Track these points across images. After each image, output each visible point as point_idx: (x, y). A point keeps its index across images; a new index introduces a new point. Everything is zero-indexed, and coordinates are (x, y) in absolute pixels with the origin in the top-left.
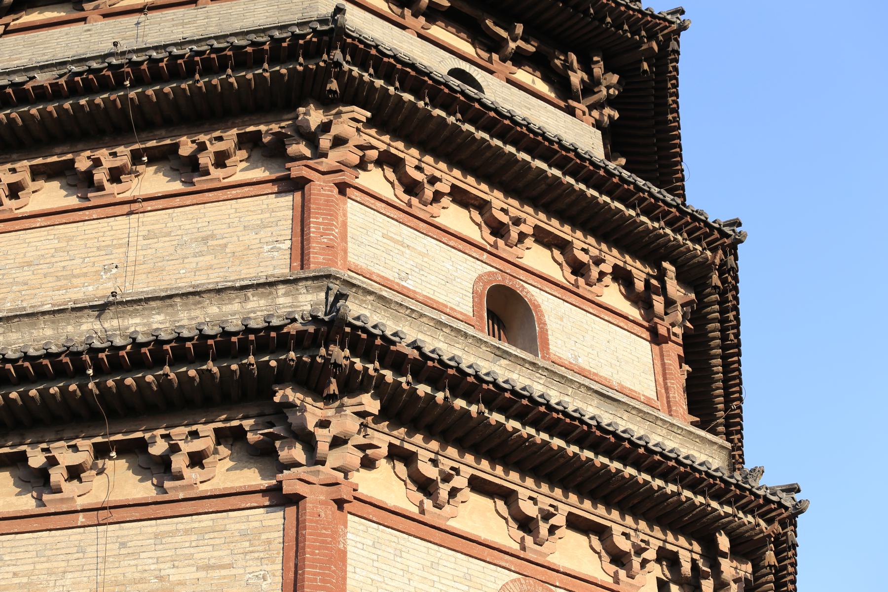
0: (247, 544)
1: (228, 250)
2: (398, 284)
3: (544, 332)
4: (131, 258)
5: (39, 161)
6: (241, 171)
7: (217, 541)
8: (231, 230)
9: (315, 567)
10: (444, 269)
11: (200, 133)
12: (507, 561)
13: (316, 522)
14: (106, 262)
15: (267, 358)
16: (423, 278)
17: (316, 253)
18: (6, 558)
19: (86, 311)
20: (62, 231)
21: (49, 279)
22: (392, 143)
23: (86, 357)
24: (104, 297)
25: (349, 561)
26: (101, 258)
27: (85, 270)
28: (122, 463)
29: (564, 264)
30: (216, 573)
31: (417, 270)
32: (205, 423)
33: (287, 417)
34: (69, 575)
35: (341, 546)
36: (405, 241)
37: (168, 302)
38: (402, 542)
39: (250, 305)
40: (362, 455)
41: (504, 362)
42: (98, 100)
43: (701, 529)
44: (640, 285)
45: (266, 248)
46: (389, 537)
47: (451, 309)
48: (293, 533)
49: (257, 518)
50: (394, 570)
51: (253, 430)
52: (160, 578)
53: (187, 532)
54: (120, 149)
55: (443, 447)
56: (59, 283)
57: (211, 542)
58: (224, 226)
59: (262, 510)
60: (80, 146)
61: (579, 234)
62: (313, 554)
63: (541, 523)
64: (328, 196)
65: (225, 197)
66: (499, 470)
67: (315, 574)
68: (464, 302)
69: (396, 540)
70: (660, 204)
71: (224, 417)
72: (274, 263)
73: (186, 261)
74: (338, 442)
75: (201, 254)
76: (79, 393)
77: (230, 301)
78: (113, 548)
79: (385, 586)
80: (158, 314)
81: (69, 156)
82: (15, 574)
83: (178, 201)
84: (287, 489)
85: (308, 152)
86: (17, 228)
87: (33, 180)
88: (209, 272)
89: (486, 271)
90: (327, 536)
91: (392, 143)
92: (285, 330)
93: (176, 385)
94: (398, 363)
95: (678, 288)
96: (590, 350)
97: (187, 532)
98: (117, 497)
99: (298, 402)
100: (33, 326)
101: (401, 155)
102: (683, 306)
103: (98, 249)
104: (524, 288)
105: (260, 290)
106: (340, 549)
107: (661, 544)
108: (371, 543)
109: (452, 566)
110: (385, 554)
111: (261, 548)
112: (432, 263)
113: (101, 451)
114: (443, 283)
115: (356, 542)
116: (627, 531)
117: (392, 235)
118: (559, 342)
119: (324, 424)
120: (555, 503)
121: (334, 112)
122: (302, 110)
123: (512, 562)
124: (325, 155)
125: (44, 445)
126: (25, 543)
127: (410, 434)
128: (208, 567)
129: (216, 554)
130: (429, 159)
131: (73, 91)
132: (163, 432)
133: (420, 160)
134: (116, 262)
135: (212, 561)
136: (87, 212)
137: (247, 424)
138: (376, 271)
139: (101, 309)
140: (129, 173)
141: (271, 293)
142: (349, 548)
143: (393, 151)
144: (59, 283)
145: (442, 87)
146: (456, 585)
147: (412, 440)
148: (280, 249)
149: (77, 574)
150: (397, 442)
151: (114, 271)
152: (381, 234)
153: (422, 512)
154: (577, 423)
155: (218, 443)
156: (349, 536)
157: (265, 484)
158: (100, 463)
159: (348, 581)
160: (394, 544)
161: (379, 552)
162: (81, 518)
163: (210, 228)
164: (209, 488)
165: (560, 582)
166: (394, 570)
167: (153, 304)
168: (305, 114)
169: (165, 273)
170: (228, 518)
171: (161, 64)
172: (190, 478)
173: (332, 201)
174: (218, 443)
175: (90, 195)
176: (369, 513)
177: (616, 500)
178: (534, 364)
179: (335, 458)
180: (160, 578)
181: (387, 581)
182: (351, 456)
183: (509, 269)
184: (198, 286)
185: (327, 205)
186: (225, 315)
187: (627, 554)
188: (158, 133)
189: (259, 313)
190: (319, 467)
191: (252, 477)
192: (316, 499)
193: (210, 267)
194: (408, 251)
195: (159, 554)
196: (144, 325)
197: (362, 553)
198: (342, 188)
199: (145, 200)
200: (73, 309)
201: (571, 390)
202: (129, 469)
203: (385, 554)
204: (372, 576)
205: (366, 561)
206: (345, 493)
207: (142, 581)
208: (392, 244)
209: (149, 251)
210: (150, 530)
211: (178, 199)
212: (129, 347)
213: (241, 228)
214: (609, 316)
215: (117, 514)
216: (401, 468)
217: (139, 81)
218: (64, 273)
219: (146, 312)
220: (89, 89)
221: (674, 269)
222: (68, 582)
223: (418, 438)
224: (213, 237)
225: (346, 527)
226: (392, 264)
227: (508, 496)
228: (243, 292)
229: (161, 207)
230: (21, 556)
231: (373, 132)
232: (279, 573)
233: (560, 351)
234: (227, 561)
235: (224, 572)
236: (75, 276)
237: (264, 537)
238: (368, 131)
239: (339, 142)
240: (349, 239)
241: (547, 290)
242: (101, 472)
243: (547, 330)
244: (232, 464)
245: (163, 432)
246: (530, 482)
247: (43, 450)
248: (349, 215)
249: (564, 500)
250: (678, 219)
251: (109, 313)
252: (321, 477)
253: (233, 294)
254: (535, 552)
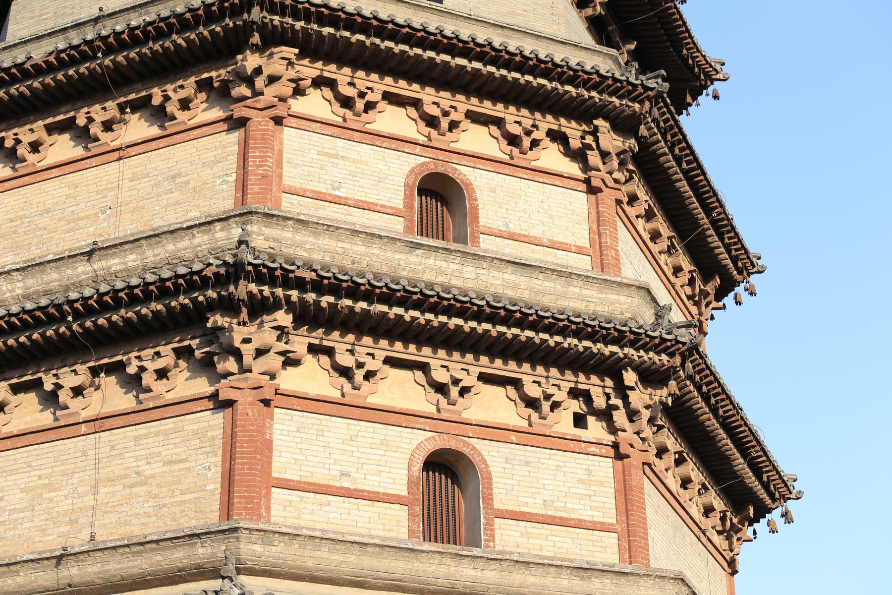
0: (198, 441)
1: (190, 186)
2: (330, 195)
3: (475, 208)
4: (119, 200)
5: (50, 120)
6: (203, 111)
7: (177, 440)
8: (193, 167)
9: (243, 458)
10: (376, 170)
11: (167, 83)
12: (422, 424)
13: (245, 421)
14: (103, 205)
15: (196, 294)
16: (356, 183)
17: (253, 185)
18: (34, 464)
19: (79, 257)
20: (71, 179)
21: (63, 223)
22: (324, 68)
23: (66, 307)
24: (89, 245)
25: (274, 447)
26: (99, 201)
27: (87, 213)
28: (112, 379)
29: (500, 138)
30: (176, 467)
31: (350, 177)
32: (165, 345)
33: (219, 338)
34: (76, 475)
35: (268, 437)
36: (340, 153)
37: (137, 244)
38: (324, 423)
39: (197, 241)
40: (283, 359)
41: (418, 252)
42: (82, 70)
43: (611, 369)
44: (575, 144)
45: (218, 181)
46: (312, 421)
47: (382, 206)
48: (229, 430)
49: (205, 419)
50: (316, 448)
52: (138, 473)
53: (157, 434)
54: (110, 104)
55: (359, 339)
56: (69, 226)
57: (173, 441)
58: (188, 164)
59: (209, 412)
60: (79, 104)
61: (512, 109)
62: (242, 447)
63: (451, 387)
64: (265, 130)
65: (189, 138)
66: (412, 348)
67: (244, 464)
68: (396, 196)
69: (318, 422)
70: (581, 73)
71: (178, 338)
72: (224, 194)
73: (160, 198)
74: (260, 353)
75: (170, 191)
76: (68, 333)
77: (182, 238)
78: (105, 451)
79: (307, 463)
80: (131, 254)
81: (72, 114)
82: (40, 477)
83: (154, 144)
84: (222, 396)
85: (247, 92)
86: (38, 179)
87: (50, 135)
88: (176, 207)
89: (419, 162)
90: (253, 431)
91: (324, 68)
92: (204, 273)
93: (136, 321)
94: (301, 284)
95: (615, 137)
96: (522, 214)
97: (157, 434)
98: (108, 410)
99: (226, 325)
100: (43, 272)
101: (333, 76)
102: (618, 155)
103: (97, 193)
104: (455, 169)
105: (202, 228)
106: (266, 440)
107: (573, 385)
108: (295, 429)
109: (371, 435)
110: (309, 436)
111: (207, 444)
112: (364, 167)
113: (95, 372)
114: (375, 183)
115: (282, 430)
116: (538, 379)
117: (327, 151)
118: (491, 213)
119: (247, 341)
120: (466, 367)
121: (267, 53)
122: (239, 57)
123: (426, 424)
124: (262, 94)
125: (54, 372)
126: (46, 451)
127: (327, 333)
128: (172, 462)
129: (176, 451)
130: (361, 74)
131: (63, 65)
132: (136, 354)
133: (352, 77)
134: (109, 204)
135: (174, 457)
136: (88, 161)
137: (194, 343)
138: (310, 188)
139: (89, 254)
140: (119, 122)
141: (210, 230)
142: (275, 437)
143: (326, 74)
144: (69, 226)
145: (356, 17)
146: (374, 451)
147: (329, 337)
148: (228, 181)
149: (81, 474)
150: (317, 342)
151: (108, 212)
152: (315, 152)
153: (343, 395)
154: (468, 305)
155: (178, 358)
156: (275, 426)
158: (97, 380)
159: (274, 464)
160: (317, 427)
161: (302, 435)
162: (84, 428)
163: (178, 167)
164: (173, 396)
165: (473, 433)
166: (316, 448)
167: (126, 247)
168: (242, 60)
169: (144, 210)
170: (185, 420)
171: (123, 36)
172: (157, 390)
173: (268, 134)
174: (178, 358)
175: (90, 146)
176: (293, 405)
177: (526, 354)
178: (447, 249)
179: (259, 366)
180: (138, 473)
181: (311, 458)
182: (273, 361)
183: (442, 156)
184: (156, 229)
185: (263, 139)
186: (179, 250)
187: (538, 399)
188: (135, 86)
189: (204, 247)
190: (248, 374)
191: (202, 386)
192: (245, 400)
193: (177, 203)
194: (341, 162)
195: (138, 453)
196: (122, 263)
197: (288, 438)
198: (278, 121)
199: (128, 147)
200: (69, 257)
201: (485, 264)
202: (117, 384)
203: (309, 436)
204: (296, 457)
205: (291, 445)
206: (268, 394)
207: (126, 476)
208: (327, 159)
209: (134, 192)
210: (131, 434)
211: (154, 143)
212: (95, 296)
213: (200, 165)
214: (544, 177)
215: (108, 423)
216: (325, 360)
217: (109, 50)
218: (72, 217)
219: (122, 254)
220: (73, 62)
221: (607, 125)
222: (76, 481)
223: (336, 335)
224: (179, 175)
225: (272, 419)
226: (325, 177)
227: (424, 368)
228: (190, 231)
229: (141, 151)
230: (43, 462)
231: (306, 62)
232: (220, 464)
233: (491, 221)
234: (184, 456)
235: (182, 466)
236: (80, 219)
237: (210, 434)
238: (301, 62)
239: (273, 79)
240: (285, 164)
241: (480, 166)
242: (98, 388)
243: (477, 205)
244: (189, 374)
245: (136, 354)
246: (442, 353)
247: (54, 375)
248: (285, 142)
249: (475, 363)
250: (601, 83)
251: (95, 257)
252: (250, 382)
253: (183, 233)
254: (449, 411)
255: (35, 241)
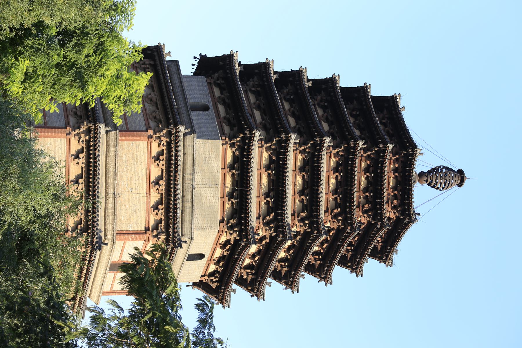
5: (164, 171)
51: (81, 227)
75: (132, 210)
137: (82, 226)
157: (70, 229)
255: (128, 167)
